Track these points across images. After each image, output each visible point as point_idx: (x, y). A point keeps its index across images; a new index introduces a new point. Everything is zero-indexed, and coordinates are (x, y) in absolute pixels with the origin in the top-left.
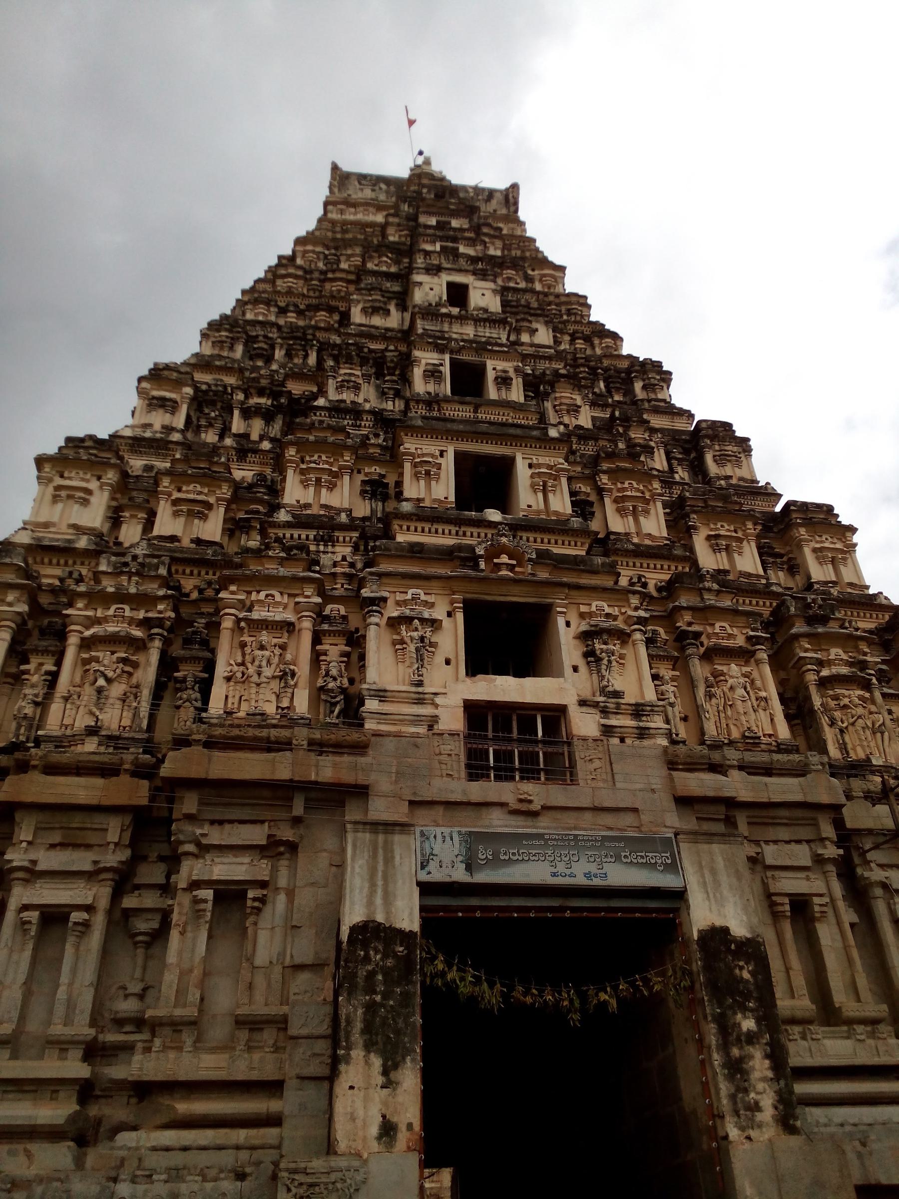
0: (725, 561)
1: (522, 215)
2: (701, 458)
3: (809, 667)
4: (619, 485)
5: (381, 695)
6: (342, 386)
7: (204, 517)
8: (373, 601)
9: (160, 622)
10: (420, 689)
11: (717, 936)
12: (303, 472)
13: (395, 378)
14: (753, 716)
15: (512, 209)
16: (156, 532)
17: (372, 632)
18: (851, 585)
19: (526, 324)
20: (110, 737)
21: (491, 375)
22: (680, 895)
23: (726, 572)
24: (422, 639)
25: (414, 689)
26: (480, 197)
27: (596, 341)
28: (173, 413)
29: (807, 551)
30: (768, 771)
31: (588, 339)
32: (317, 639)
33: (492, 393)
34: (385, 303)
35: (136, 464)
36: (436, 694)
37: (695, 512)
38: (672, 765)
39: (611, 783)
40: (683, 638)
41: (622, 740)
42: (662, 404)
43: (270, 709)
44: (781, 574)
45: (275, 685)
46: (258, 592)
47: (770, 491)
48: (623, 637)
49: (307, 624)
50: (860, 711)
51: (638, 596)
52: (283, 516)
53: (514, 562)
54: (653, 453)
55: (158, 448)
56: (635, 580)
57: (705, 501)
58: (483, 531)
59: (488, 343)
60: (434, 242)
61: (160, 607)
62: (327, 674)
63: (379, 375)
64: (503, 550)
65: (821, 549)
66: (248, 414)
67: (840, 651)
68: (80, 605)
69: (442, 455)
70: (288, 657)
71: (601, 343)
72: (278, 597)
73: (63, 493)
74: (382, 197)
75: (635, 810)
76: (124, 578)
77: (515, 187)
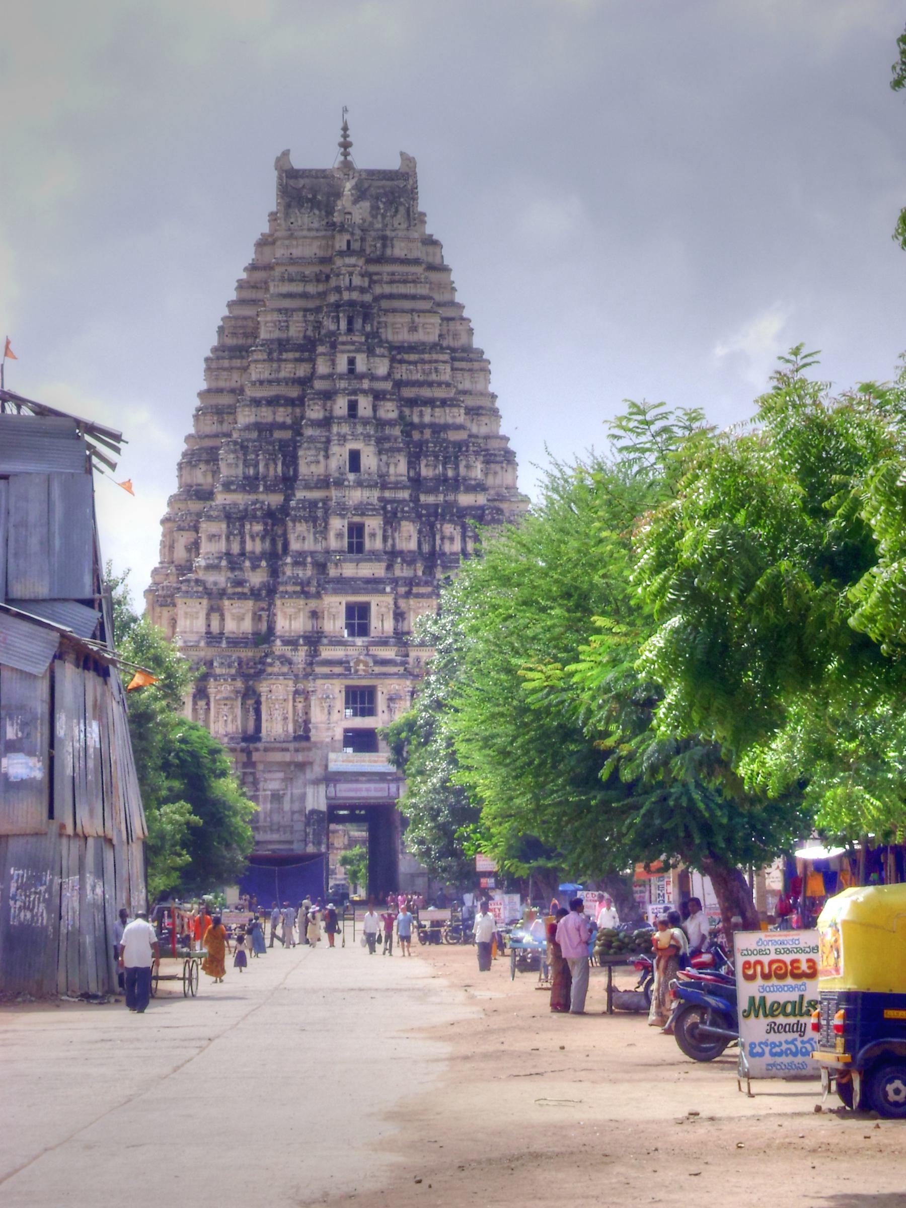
19: (392, 460)
21: (367, 531)
32: (294, 701)
33: (368, 545)
42: (473, 482)
48: (400, 698)
49: (291, 697)
52: (278, 642)
66: (253, 538)
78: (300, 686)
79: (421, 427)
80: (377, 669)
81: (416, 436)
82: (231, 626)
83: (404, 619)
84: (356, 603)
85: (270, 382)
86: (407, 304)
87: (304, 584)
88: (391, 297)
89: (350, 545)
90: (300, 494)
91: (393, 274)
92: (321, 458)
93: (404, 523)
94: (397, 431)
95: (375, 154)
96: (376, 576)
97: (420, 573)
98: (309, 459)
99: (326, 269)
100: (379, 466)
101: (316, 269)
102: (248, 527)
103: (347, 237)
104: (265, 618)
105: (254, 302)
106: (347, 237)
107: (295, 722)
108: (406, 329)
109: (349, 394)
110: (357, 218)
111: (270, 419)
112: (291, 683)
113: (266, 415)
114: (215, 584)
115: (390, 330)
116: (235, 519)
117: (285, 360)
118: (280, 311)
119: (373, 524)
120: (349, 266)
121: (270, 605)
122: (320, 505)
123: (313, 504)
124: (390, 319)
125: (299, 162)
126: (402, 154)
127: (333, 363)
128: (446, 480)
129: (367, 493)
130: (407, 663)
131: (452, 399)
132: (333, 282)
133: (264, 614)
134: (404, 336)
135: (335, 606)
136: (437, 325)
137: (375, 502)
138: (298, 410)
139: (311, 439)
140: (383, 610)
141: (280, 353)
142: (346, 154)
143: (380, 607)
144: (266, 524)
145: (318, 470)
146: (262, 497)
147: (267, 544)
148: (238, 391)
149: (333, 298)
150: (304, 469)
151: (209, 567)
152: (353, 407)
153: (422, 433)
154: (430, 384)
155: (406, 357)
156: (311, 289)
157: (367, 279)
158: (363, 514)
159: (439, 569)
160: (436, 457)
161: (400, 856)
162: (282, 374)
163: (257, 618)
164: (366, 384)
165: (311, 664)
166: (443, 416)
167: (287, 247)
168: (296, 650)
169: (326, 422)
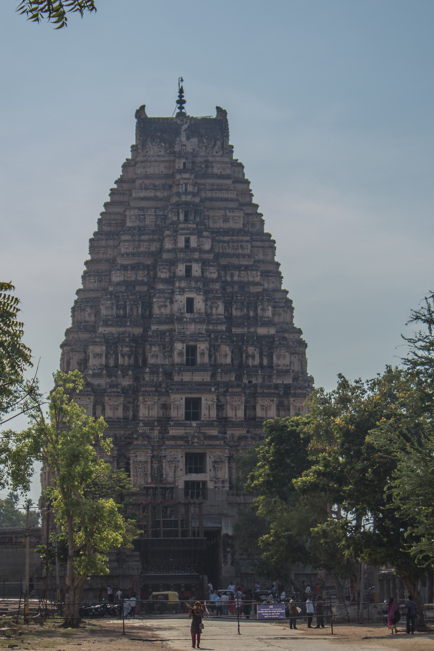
2: (272, 353)
8: (164, 456)
9: (116, 457)
11: (227, 535)
19: (215, 305)
21: (198, 351)
22: (221, 528)
24: (175, 466)
26: (210, 146)
32: (152, 462)
33: (199, 360)
34: (165, 302)
38: (228, 495)
42: (266, 319)
48: (222, 462)
49: (149, 460)
52: (141, 424)
60: (183, 263)
64: (196, 437)
66: (123, 356)
69: (181, 399)
71: (251, 274)
74: (162, 153)
78: (156, 453)
79: (233, 283)
80: (206, 442)
81: (229, 289)
83: (223, 409)
84: (192, 399)
85: (133, 254)
86: (223, 204)
87: (158, 386)
88: (211, 199)
89: (187, 360)
90: (154, 327)
91: (213, 185)
92: (168, 303)
93: (222, 346)
94: (217, 286)
95: (199, 108)
96: (205, 380)
97: (233, 379)
98: (160, 304)
99: (170, 182)
100: (206, 309)
101: (163, 181)
102: (120, 348)
103: (183, 161)
104: (131, 408)
105: (121, 203)
106: (183, 161)
108: (221, 220)
109: (186, 262)
110: (189, 149)
111: (133, 279)
112: (150, 451)
113: (131, 276)
114: (99, 385)
115: (211, 221)
116: (111, 343)
117: (142, 240)
118: (139, 209)
119: (202, 347)
120: (185, 179)
121: (134, 400)
122: (168, 334)
123: (163, 333)
124: (211, 213)
125: (150, 113)
126: (218, 108)
127: (176, 242)
128: (249, 318)
129: (199, 326)
130: (226, 438)
131: (251, 266)
132: (175, 190)
133: (131, 406)
134: (220, 224)
135: (178, 400)
136: (242, 218)
137: (204, 332)
138: (151, 273)
139: (162, 291)
140: (210, 403)
141: (140, 235)
142: (181, 108)
143: (208, 402)
144: (131, 347)
145: (166, 311)
146: (129, 329)
147: (132, 361)
148: (112, 262)
149: (174, 200)
150: (156, 311)
151: (94, 375)
152: (188, 270)
153: (233, 287)
154: (238, 256)
155: (222, 238)
156: (159, 194)
157: (196, 188)
158: (196, 340)
159: (246, 376)
160: (242, 303)
161: (223, 566)
162: (141, 249)
163: (126, 409)
164: (196, 255)
165: (163, 438)
166: (247, 277)
167: (144, 167)
168: (153, 429)
169: (170, 281)
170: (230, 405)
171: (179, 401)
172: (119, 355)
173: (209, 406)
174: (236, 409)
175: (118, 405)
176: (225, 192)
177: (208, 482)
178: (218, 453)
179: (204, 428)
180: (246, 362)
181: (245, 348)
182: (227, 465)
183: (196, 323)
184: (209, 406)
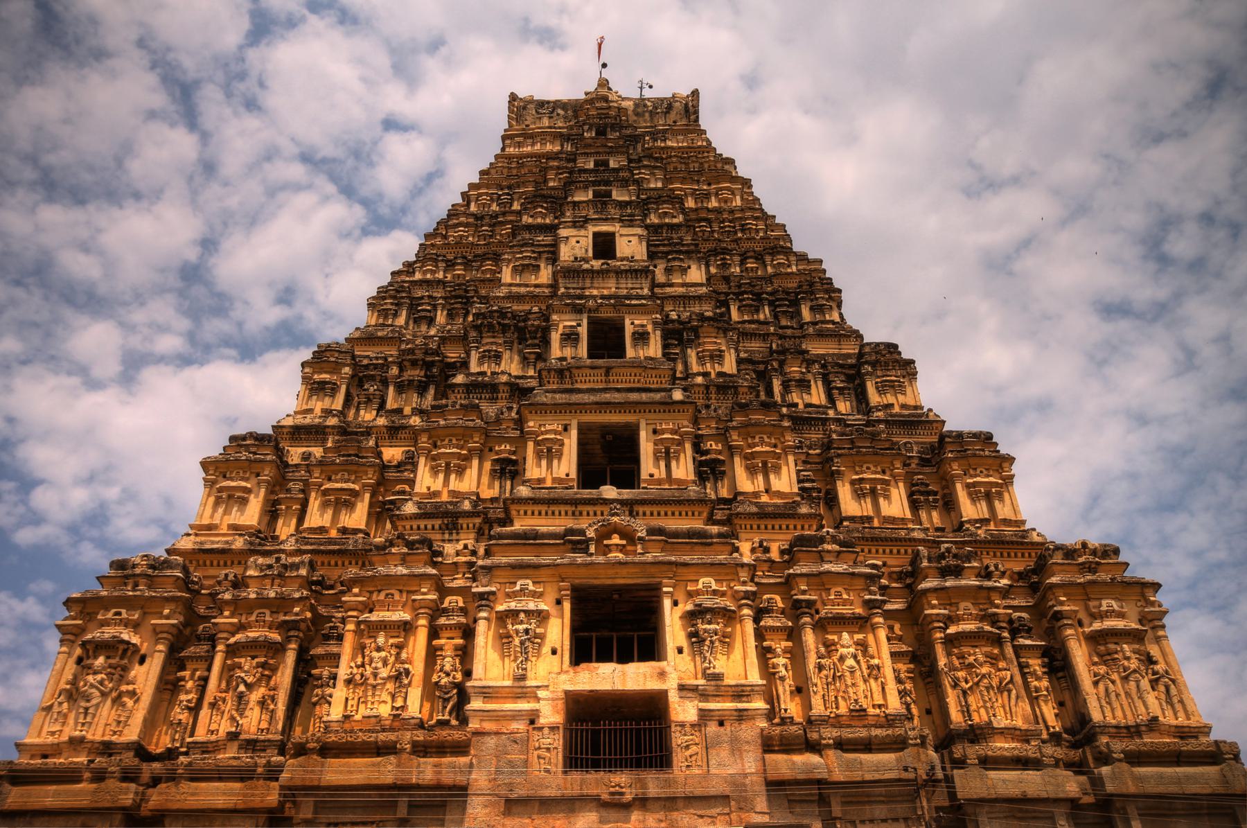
0: (870, 506)
1: (703, 124)
3: (936, 625)
4: (750, 441)
5: (488, 693)
6: (483, 357)
7: (350, 506)
8: (482, 596)
9: (293, 625)
10: (522, 684)
12: (434, 459)
13: (537, 341)
14: (862, 686)
15: (692, 117)
16: (306, 525)
17: (481, 627)
18: (1006, 522)
20: (249, 742)
21: (629, 330)
23: (869, 519)
25: (516, 684)
27: (768, 259)
28: (333, 396)
29: (959, 486)
30: (867, 746)
31: (759, 258)
32: (434, 633)
33: (630, 352)
35: (295, 454)
36: (538, 687)
37: (839, 456)
38: (768, 745)
39: (705, 768)
40: (797, 609)
41: (721, 724)
43: (385, 710)
44: (935, 514)
45: (390, 686)
46: (379, 591)
47: (931, 417)
50: (984, 670)
51: (746, 569)
52: (410, 508)
53: (624, 542)
54: (809, 387)
55: (317, 433)
56: (756, 545)
57: (852, 441)
58: (599, 509)
59: (629, 297)
61: (297, 609)
62: (441, 670)
63: (522, 340)
64: (616, 530)
65: (974, 485)
66: (401, 388)
67: (970, 605)
68: (227, 613)
69: (566, 429)
70: (404, 655)
72: (397, 597)
73: (224, 495)
75: (728, 797)
76: (268, 581)
77: (695, 93)
82: (317, 517)
84: (606, 429)
107: (431, 691)
109: (594, 183)
117: (502, 223)
141: (497, 216)
144: (428, 366)
150: (507, 276)
154: (736, 241)
160: (758, 297)
163: (382, 512)
170: (746, 457)
171: (556, 432)
172: (391, 389)
173: (667, 452)
174: (765, 468)
175: (355, 494)
176: (697, 165)
177: (673, 697)
178: (707, 581)
179: (648, 509)
180: (783, 396)
181: (775, 364)
182: (749, 626)
183: (619, 273)
184: (667, 452)
